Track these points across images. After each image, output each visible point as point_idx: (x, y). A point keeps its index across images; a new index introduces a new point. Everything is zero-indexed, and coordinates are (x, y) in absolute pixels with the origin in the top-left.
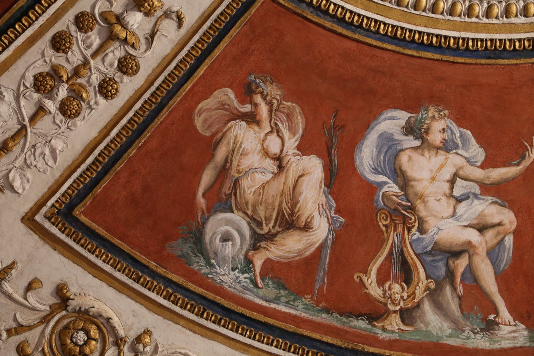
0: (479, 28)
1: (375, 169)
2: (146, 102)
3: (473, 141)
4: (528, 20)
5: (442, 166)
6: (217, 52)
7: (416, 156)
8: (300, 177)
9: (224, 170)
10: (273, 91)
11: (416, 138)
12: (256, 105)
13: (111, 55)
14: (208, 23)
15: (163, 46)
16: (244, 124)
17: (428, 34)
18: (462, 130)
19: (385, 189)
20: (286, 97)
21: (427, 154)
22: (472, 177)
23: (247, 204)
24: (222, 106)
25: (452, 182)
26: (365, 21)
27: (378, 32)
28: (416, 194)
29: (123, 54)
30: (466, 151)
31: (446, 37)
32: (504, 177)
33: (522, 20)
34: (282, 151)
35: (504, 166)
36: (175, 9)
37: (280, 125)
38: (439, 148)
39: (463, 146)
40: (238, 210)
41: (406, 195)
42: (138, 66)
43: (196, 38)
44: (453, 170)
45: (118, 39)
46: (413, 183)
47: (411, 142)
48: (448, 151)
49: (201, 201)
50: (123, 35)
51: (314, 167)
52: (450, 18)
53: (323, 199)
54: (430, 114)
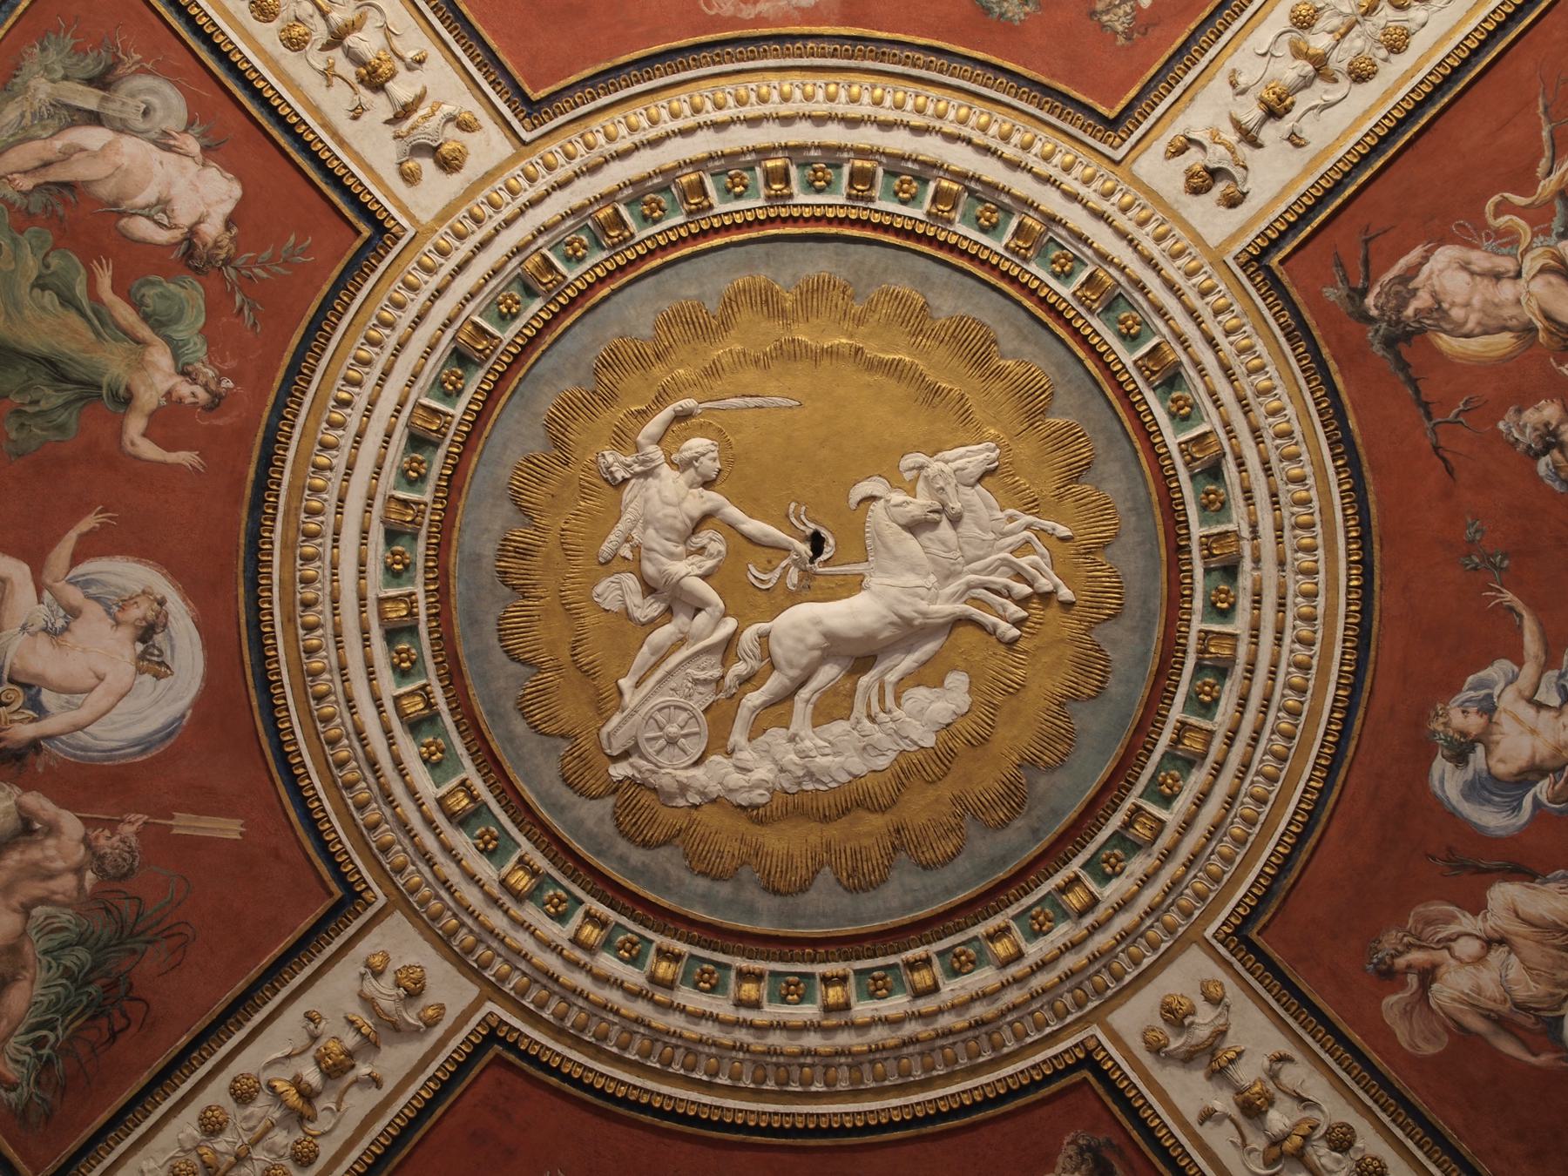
0: (1326, 656)
1: (1514, 810)
2: (1394, 1121)
3: (1482, 674)
4: (1322, 592)
5: (1516, 718)
6: (1331, 1013)
7: (1499, 752)
8: (1517, 916)
9: (1500, 1022)
10: (1390, 940)
11: (1473, 750)
12: (1409, 966)
13: (1324, 1160)
14: (1290, 1021)
15: (1316, 1086)
16: (1435, 986)
17: (1330, 723)
18: (1466, 687)
19: (1543, 798)
20: (1401, 925)
21: (1496, 738)
22: (1535, 680)
23: (1552, 995)
24: (1407, 1013)
25: (1540, 706)
26: (1303, 806)
27: (1320, 790)
28: (1554, 757)
29: (1323, 1143)
30: (1496, 683)
31: (1335, 700)
32: (1537, 636)
33: (1321, 601)
34: (1478, 937)
35: (1521, 635)
36: (1267, 1063)
37: (1440, 936)
38: (1490, 720)
39: (1488, 687)
40: (1560, 1008)
41: (1554, 771)
42: (1343, 1125)
43: (1309, 1039)
44: (1523, 704)
45: (1302, 1147)
46: (1537, 759)
47: (1478, 757)
48: (1494, 709)
49: (1544, 1059)
50: (1297, 1140)
51: (1503, 894)
52: (1309, 692)
53: (1552, 886)
54: (1440, 728)
